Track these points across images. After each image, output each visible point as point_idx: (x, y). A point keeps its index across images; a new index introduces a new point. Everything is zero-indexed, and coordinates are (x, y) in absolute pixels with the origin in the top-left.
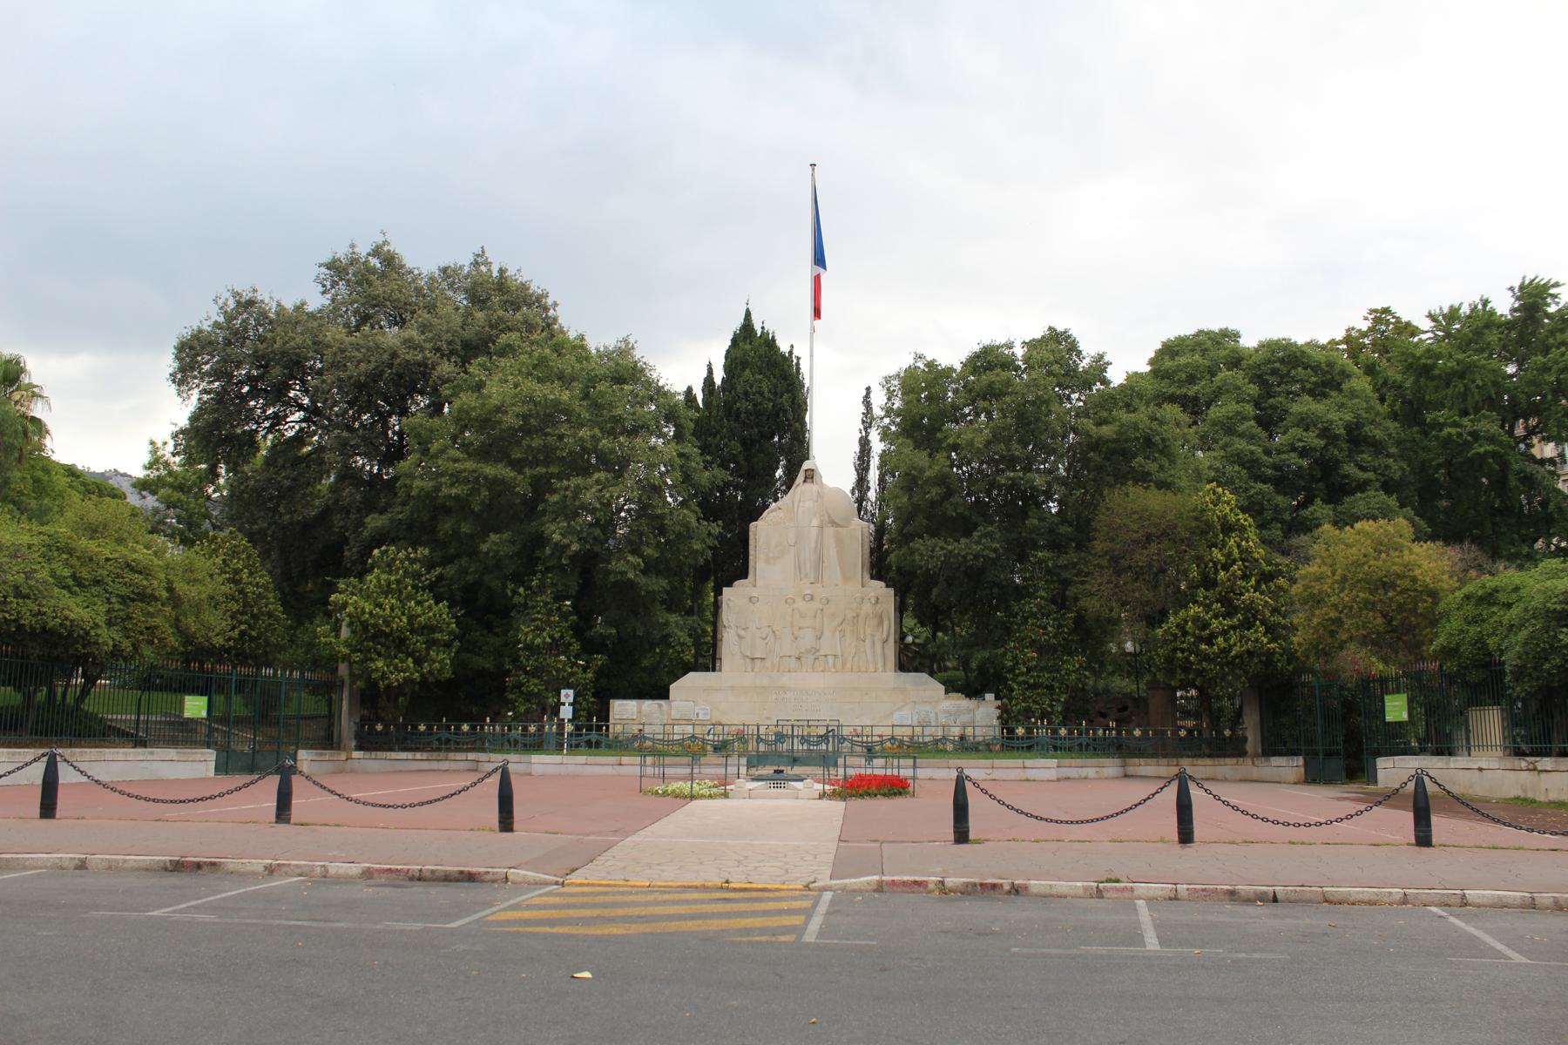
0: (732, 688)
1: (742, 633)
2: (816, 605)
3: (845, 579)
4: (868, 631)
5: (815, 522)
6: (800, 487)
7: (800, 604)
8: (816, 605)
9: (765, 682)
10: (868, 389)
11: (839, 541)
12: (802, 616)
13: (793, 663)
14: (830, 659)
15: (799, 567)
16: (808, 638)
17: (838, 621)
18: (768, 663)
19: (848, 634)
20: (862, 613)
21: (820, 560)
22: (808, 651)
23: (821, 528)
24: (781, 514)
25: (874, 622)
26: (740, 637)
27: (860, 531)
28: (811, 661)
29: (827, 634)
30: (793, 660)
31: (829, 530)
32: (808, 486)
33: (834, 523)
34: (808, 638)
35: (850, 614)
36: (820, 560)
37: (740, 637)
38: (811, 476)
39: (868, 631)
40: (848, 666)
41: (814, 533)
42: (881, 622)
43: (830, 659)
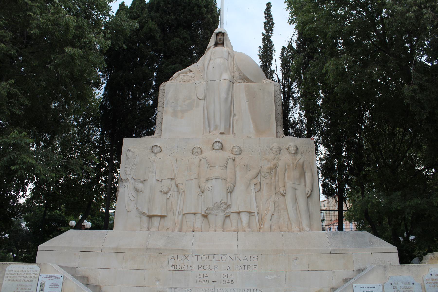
0: (117, 251)
1: (140, 186)
2: (227, 154)
3: (259, 131)
4: (289, 184)
5: (226, 76)
6: (213, 55)
7: (208, 154)
8: (227, 154)
9: (161, 243)
10: (269, 5)
11: (252, 97)
12: (210, 166)
13: (198, 221)
14: (244, 217)
15: (208, 121)
16: (217, 192)
17: (253, 173)
18: (168, 222)
19: (265, 188)
20: (281, 165)
21: (230, 113)
22: (217, 207)
23: (232, 83)
24: (191, 74)
25: (296, 174)
26: (138, 191)
27: (269, 91)
28: (221, 215)
29: (240, 188)
30: (199, 219)
31: (240, 86)
32: (219, 49)
33: (245, 79)
34: (217, 192)
35: (267, 166)
36: (230, 113)
37: (138, 191)
38: (222, 39)
39: (289, 184)
40: (266, 226)
41: (224, 85)
42: (302, 174)
43: (244, 217)
